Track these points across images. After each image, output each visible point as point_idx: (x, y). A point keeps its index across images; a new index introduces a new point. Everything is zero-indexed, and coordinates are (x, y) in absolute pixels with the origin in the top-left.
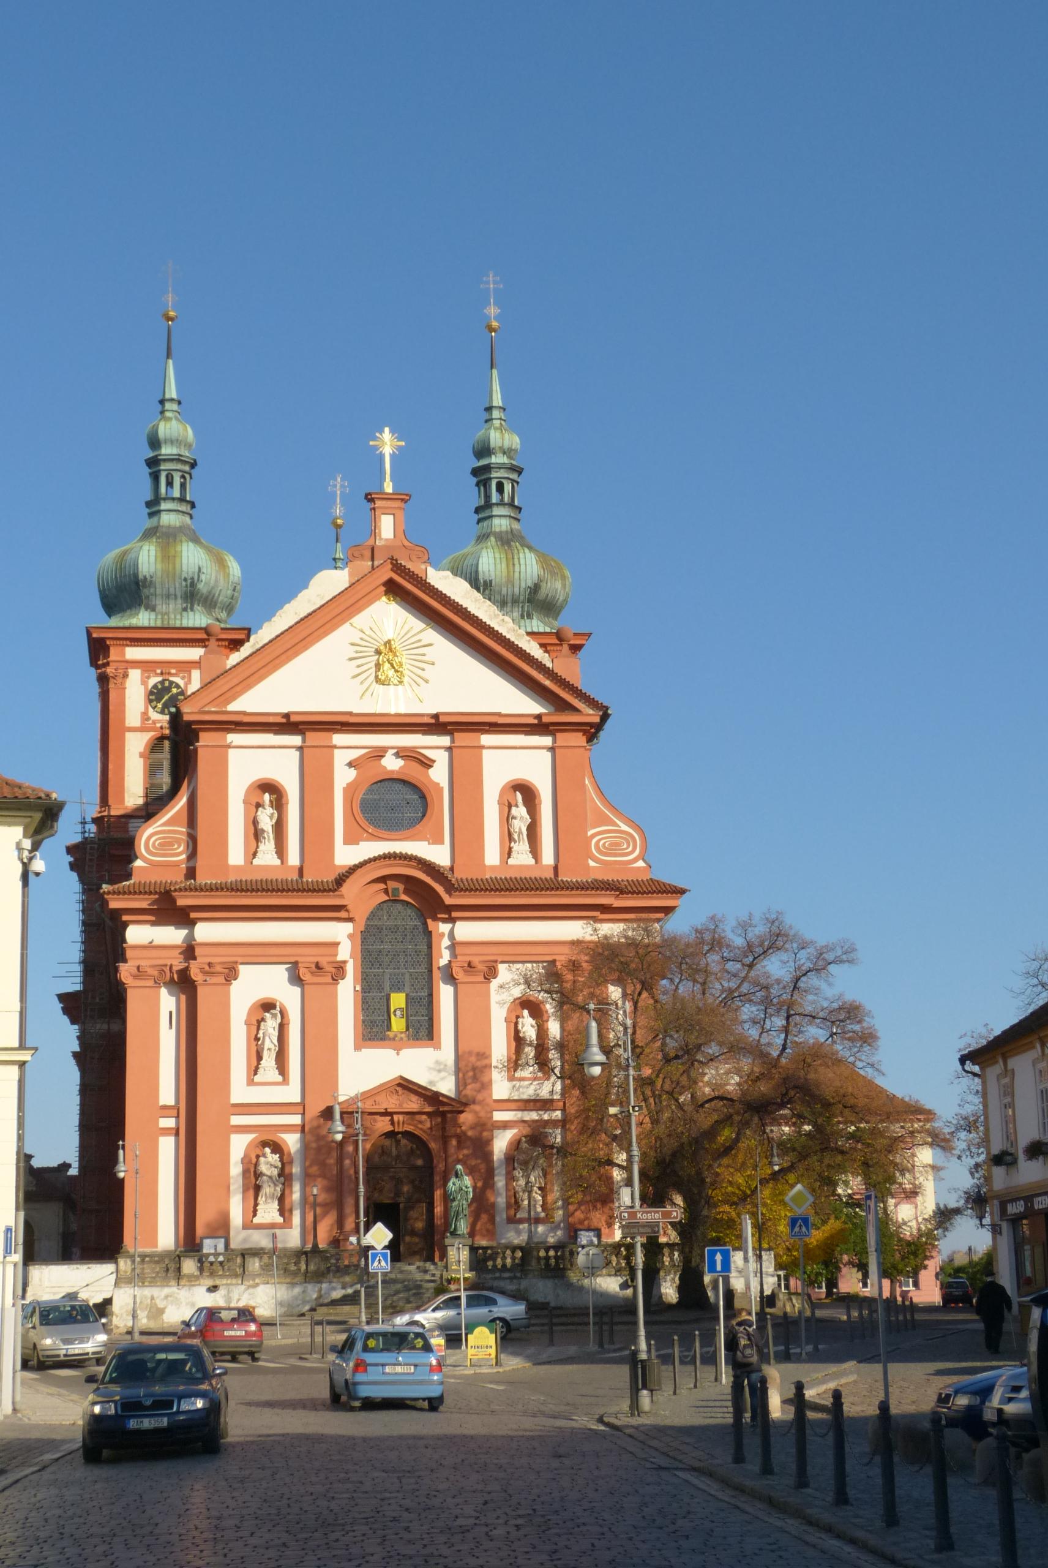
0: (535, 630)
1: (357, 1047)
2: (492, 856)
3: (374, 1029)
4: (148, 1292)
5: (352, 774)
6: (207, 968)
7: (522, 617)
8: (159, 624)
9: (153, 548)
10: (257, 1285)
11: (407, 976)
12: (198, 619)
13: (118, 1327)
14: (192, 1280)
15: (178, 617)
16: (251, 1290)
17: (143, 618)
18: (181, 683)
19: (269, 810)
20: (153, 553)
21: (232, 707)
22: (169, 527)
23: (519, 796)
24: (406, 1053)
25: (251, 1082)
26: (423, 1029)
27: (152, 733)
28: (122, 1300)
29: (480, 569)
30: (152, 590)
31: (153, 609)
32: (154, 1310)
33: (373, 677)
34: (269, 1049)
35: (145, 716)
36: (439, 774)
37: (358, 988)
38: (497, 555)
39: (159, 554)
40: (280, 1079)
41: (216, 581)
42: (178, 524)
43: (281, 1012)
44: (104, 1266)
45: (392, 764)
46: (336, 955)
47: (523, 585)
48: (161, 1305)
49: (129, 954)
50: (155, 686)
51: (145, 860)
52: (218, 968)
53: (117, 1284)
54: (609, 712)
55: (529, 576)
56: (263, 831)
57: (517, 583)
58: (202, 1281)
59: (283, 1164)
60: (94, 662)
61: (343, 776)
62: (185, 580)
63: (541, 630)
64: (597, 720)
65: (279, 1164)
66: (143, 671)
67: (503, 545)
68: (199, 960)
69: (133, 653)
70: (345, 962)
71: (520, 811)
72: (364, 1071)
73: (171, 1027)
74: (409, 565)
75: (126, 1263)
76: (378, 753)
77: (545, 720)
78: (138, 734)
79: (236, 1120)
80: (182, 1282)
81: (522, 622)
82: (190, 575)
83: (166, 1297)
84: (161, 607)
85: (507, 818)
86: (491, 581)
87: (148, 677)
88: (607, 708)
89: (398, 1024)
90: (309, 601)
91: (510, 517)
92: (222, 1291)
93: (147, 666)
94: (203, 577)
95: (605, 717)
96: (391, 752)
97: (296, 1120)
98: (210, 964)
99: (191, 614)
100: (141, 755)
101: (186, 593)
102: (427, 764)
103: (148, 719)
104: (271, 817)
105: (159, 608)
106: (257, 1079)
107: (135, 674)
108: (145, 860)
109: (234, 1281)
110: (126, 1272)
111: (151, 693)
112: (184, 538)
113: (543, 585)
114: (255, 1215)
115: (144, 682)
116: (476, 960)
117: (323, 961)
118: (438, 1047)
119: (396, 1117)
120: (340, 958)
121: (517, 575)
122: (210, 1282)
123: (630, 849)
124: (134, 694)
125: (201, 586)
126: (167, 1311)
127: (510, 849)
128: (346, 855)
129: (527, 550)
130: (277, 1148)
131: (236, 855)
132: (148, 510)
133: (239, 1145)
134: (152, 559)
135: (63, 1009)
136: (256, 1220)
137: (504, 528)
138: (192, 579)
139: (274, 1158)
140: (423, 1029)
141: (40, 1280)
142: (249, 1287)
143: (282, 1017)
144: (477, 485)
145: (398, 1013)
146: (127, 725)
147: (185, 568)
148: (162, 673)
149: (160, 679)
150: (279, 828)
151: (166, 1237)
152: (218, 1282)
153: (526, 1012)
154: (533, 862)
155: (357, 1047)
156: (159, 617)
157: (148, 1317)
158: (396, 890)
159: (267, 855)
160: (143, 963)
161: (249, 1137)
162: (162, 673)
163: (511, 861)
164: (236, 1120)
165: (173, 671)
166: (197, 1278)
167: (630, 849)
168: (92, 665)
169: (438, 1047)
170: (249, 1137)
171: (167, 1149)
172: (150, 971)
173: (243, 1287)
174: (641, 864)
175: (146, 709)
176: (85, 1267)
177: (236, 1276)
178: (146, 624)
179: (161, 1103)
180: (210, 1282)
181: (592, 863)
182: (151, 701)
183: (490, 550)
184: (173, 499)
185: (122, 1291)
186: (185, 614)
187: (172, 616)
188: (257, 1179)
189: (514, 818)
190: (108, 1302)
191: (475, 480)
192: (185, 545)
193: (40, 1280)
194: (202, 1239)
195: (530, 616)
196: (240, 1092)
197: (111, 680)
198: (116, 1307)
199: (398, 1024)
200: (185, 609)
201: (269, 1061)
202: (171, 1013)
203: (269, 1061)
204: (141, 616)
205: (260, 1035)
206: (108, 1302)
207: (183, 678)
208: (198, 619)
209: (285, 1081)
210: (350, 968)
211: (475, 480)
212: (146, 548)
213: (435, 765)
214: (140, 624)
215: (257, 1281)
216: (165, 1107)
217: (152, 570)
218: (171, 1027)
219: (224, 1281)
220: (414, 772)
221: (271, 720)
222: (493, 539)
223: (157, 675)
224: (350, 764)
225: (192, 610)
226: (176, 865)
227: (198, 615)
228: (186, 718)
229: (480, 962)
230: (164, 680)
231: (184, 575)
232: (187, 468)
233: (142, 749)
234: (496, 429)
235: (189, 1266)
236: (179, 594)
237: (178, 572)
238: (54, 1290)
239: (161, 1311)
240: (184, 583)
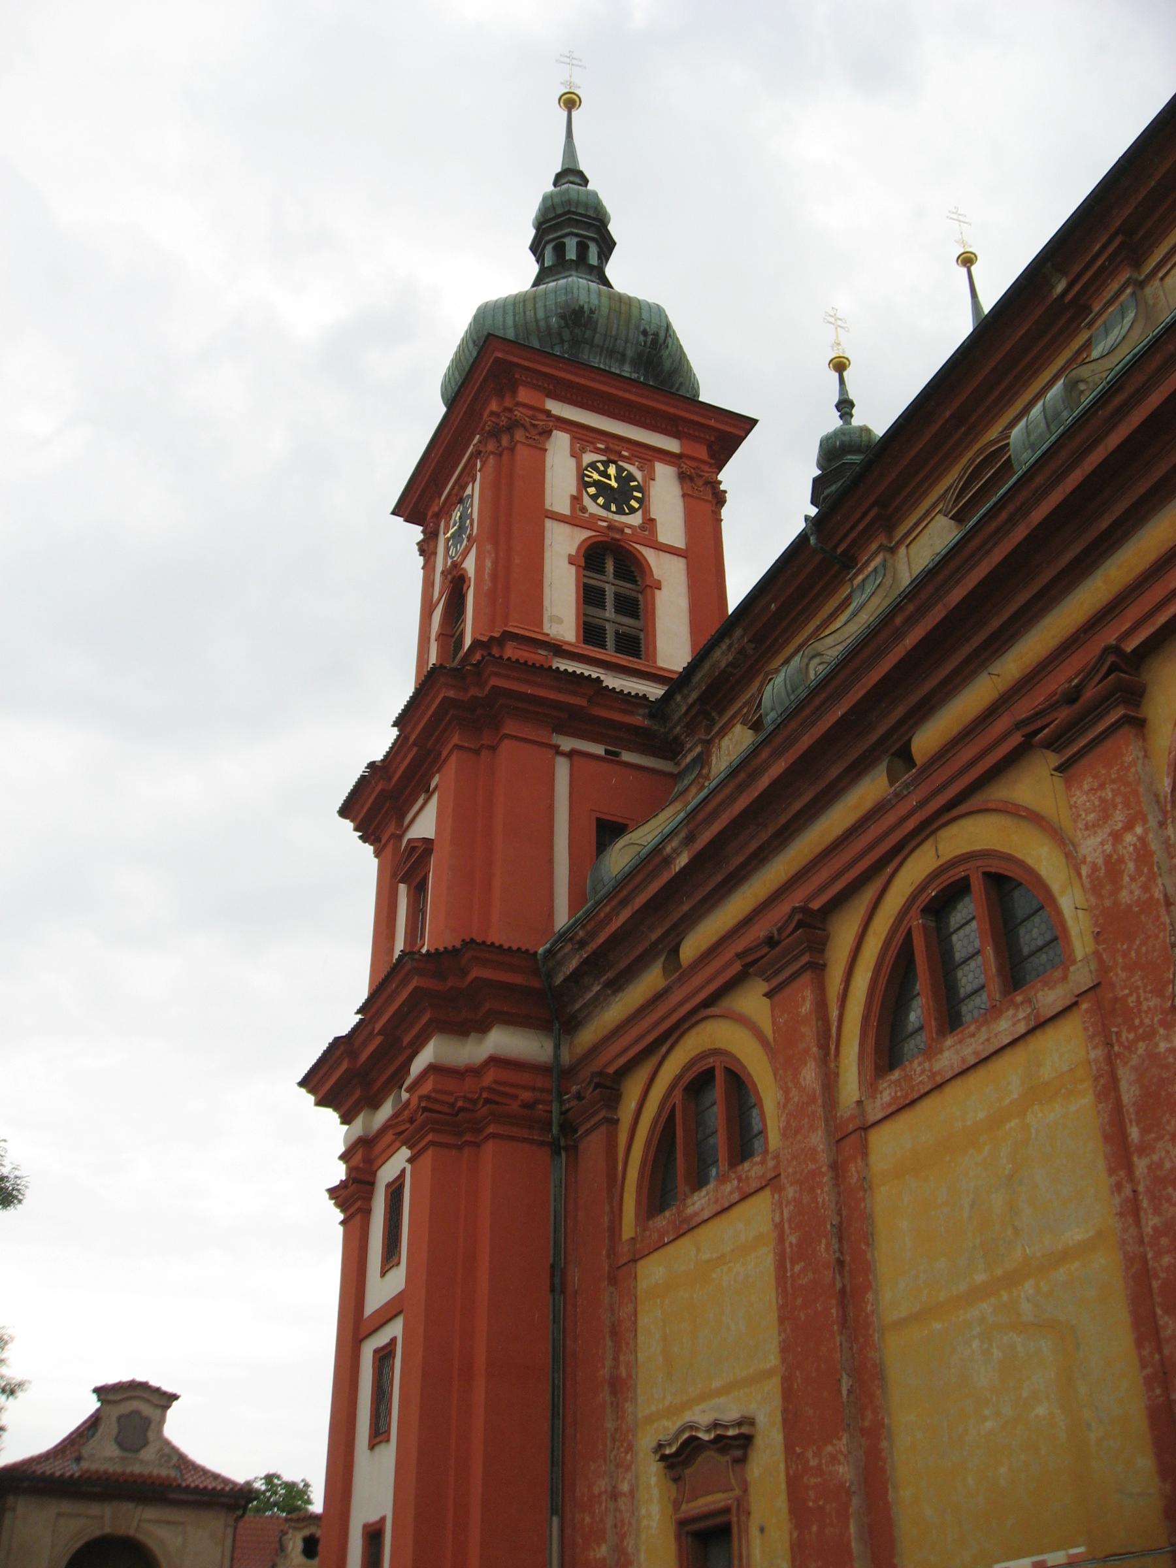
18: (638, 475)
27: (587, 534)
30: (588, 333)
35: (576, 500)
50: (593, 465)
62: (645, 333)
66: (574, 438)
69: (557, 408)
87: (583, 450)
100: (572, 561)
101: (640, 355)
103: (584, 509)
107: (560, 442)
124: (561, 470)
125: (665, 353)
138: (656, 335)
147: (645, 315)
149: (604, 458)
175: (579, 491)
197: (519, 435)
207: (640, 469)
217: (594, 301)
223: (598, 451)
236: (630, 353)
240: (642, 338)
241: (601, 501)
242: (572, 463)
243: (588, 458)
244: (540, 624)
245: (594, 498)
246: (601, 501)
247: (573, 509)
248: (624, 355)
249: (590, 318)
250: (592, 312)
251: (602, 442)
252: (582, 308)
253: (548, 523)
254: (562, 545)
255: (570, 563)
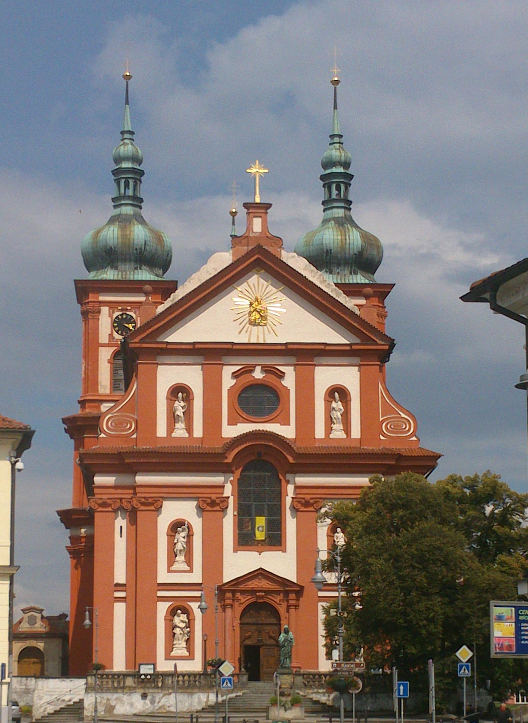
0: (359, 282)
1: (235, 551)
2: (320, 432)
3: (245, 540)
4: (106, 696)
5: (234, 382)
6: (143, 500)
7: (351, 273)
8: (120, 278)
9: (116, 229)
10: (170, 694)
11: (266, 507)
12: (145, 275)
13: (87, 716)
14: (131, 690)
15: (132, 273)
16: (166, 696)
17: (110, 274)
19: (182, 404)
20: (116, 232)
21: (159, 339)
22: (126, 215)
23: (336, 394)
24: (266, 554)
25: (169, 571)
26: (275, 540)
28: (89, 701)
29: (324, 242)
31: (116, 268)
32: (108, 706)
33: (247, 320)
34: (181, 551)
35: (111, 335)
36: (289, 380)
37: (236, 513)
38: (335, 233)
39: (120, 233)
40: (188, 568)
41: (156, 249)
42: (132, 213)
43: (188, 528)
44: (80, 680)
45: (258, 374)
46: (223, 493)
47: (351, 252)
48: (113, 704)
49: (96, 491)
50: (117, 317)
51: (105, 433)
52: (150, 500)
53: (86, 689)
54: (395, 342)
55: (355, 248)
56: (178, 415)
57: (347, 251)
58: (137, 690)
59: (189, 621)
60: (80, 301)
61: (228, 382)
62: (136, 249)
63: (363, 282)
64: (387, 347)
65: (187, 621)
66: (110, 308)
67: (339, 226)
68: (138, 495)
70: (228, 497)
71: (338, 405)
72: (238, 564)
73: (121, 536)
74: (270, 249)
75: (92, 678)
76: (249, 370)
77: (354, 347)
78: (107, 348)
79: (160, 594)
80: (125, 691)
81: (351, 276)
82: (140, 246)
83: (116, 699)
84: (121, 266)
85: (328, 410)
86: (331, 250)
87: (113, 312)
88: (393, 340)
89: (260, 535)
90: (208, 272)
91: (344, 208)
92: (149, 697)
93: (112, 305)
94: (147, 248)
95: (392, 345)
96: (258, 369)
97: (198, 594)
98: (145, 498)
99: (140, 271)
102: (281, 375)
103: (113, 338)
104: (183, 407)
105: (120, 267)
106: (173, 568)
107: (105, 310)
108: (105, 433)
109: (156, 691)
110: (91, 684)
111: (115, 322)
112: (136, 222)
113: (365, 252)
114: (172, 651)
115: (110, 316)
116: (308, 497)
117: (214, 497)
118: (284, 551)
119: (258, 594)
120: (224, 495)
121: (347, 246)
122: (142, 691)
123: (407, 429)
124: (105, 322)
126: (117, 707)
127: (331, 429)
128: (231, 432)
129: (354, 230)
130: (186, 611)
131: (161, 431)
132: (113, 204)
133: (163, 608)
134: (116, 236)
135: (61, 519)
136: (172, 654)
137: (340, 215)
138: (141, 249)
139: (184, 617)
140: (275, 540)
141: (42, 687)
142: (165, 695)
143: (189, 531)
144: (324, 186)
145: (260, 529)
146: (100, 342)
147: (136, 242)
148: (122, 310)
149: (121, 313)
150: (188, 414)
151: (119, 664)
152: (146, 691)
153: (339, 530)
154: (345, 436)
155: (235, 551)
156: (120, 273)
157: (105, 711)
158: (259, 454)
159: (180, 431)
160: (104, 497)
161: (167, 604)
162: (122, 310)
163: (331, 436)
164: (160, 594)
165: (129, 308)
166: (135, 688)
167: (407, 429)
168: (78, 303)
169: (284, 551)
170: (167, 604)
171: (120, 610)
172: (109, 501)
173: (161, 695)
174: (414, 438)
176: (69, 680)
177: (158, 687)
178: (112, 278)
179: (115, 582)
180: (142, 691)
181: (382, 438)
182: (115, 327)
183: (331, 230)
184: (129, 197)
185: (89, 695)
186: (136, 271)
187: (128, 273)
188: (173, 629)
189: (334, 409)
190: (81, 701)
191: (322, 183)
192: (136, 226)
193: (42, 687)
194: (140, 665)
195: (355, 273)
196: (163, 576)
198: (86, 704)
199: (260, 535)
200: (136, 268)
201: (181, 558)
202: (121, 527)
203: (181, 558)
204: (108, 273)
205: (176, 541)
206: (81, 701)
207: (135, 313)
208: (145, 275)
209: (191, 571)
210: (231, 501)
211: (322, 183)
212: (112, 229)
213: (286, 375)
214: (108, 278)
215: (170, 691)
216: (117, 585)
218: (121, 536)
219: (151, 691)
220: (272, 380)
221: (183, 347)
222: (333, 222)
224: (233, 373)
225: (140, 269)
226: (127, 436)
227: (144, 271)
228: (131, 345)
229: (311, 499)
230: (123, 314)
231: (136, 246)
232: (138, 177)
233: (109, 357)
234: (336, 149)
235: (129, 681)
236: (132, 259)
237: (131, 245)
238: (50, 693)
239: (113, 708)
240: (135, 252)
241: (120, 332)
242: (109, 319)
243: (115, 315)
244: (97, 391)
245: (117, 332)
246: (120, 332)
247: (109, 341)
248: (131, 260)
249: (115, 251)
250: (115, 248)
251: (120, 306)
252: (111, 248)
253: (100, 348)
254: (105, 355)
255: (109, 363)
